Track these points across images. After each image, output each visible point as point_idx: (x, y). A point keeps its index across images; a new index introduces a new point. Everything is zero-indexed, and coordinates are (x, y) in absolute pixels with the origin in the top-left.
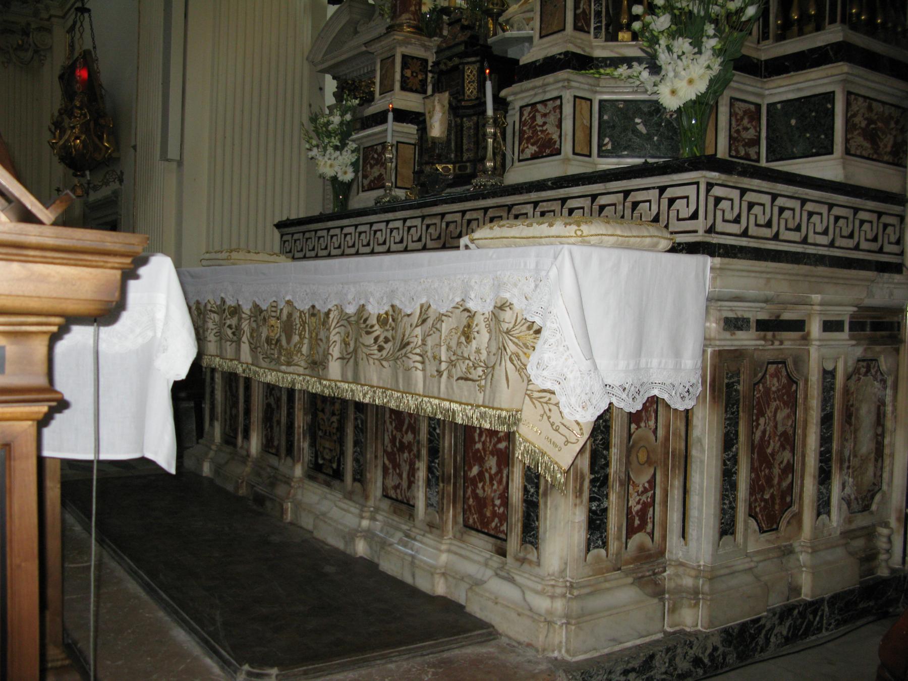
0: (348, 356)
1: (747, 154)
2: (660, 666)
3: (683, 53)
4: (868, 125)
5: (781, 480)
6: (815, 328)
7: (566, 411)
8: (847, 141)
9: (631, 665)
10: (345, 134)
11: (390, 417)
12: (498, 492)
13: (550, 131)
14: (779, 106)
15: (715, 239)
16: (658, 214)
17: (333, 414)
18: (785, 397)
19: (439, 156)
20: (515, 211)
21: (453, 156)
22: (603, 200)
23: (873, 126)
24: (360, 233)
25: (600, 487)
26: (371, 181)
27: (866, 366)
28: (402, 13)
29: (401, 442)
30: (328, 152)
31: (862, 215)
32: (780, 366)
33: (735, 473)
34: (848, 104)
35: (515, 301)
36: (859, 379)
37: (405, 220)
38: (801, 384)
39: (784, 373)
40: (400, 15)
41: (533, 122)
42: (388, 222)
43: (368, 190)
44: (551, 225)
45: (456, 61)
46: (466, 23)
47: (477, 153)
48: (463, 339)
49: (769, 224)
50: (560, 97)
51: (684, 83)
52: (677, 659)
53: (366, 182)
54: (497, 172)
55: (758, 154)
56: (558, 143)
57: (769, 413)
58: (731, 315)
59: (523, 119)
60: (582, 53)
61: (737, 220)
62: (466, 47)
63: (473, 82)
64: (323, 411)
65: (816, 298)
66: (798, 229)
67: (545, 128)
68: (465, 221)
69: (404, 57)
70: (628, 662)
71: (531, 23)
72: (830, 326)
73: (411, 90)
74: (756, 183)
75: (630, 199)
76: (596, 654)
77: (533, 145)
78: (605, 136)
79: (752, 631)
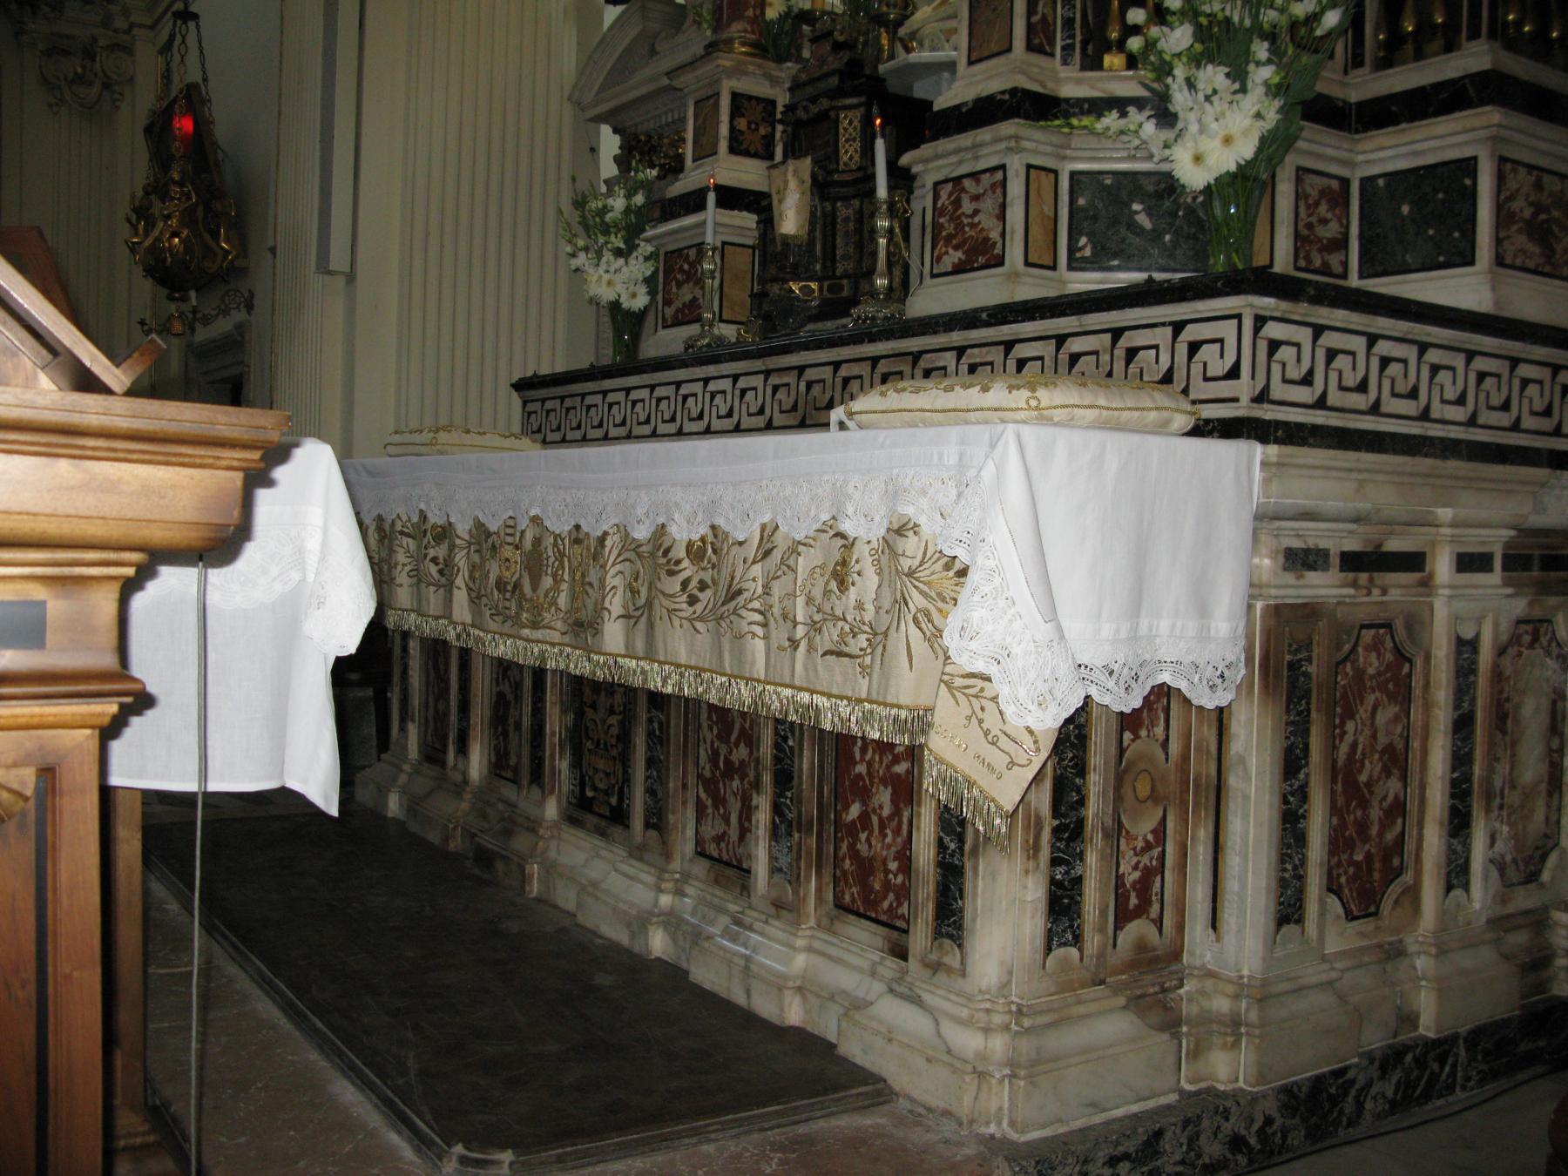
0: (637, 613)
1: (1326, 265)
2: (1173, 1149)
3: (1215, 92)
4: (1535, 215)
5: (1384, 827)
6: (1442, 566)
7: (1009, 711)
8: (1499, 241)
9: (1121, 1149)
10: (633, 229)
11: (710, 718)
12: (894, 849)
13: (984, 225)
14: (1381, 182)
15: (1268, 413)
16: (1171, 370)
17: (612, 712)
18: (1391, 686)
19: (795, 266)
20: (924, 363)
21: (818, 267)
22: (1075, 345)
23: (1543, 216)
24: (659, 400)
25: (1070, 840)
26: (678, 310)
27: (1533, 630)
28: (731, 20)
29: (728, 762)
30: (604, 259)
31: (1525, 371)
32: (1382, 631)
33: (1304, 817)
34: (1501, 178)
35: (922, 520)
36: (1520, 654)
37: (736, 378)
38: (1419, 663)
39: (1389, 644)
40: (728, 25)
41: (956, 210)
42: (706, 381)
43: (673, 325)
44: (985, 389)
45: (825, 103)
46: (841, 39)
47: (859, 262)
48: (833, 585)
49: (1362, 387)
50: (1003, 167)
51: (1216, 143)
52: (1203, 1138)
53: (669, 311)
54: (895, 295)
55: (1345, 264)
56: (999, 245)
57: (1363, 712)
58: (1297, 544)
59: (939, 204)
60: (1041, 90)
61: (1307, 380)
62: (841, 80)
63: (854, 140)
64: (593, 707)
65: (1445, 514)
66: (1413, 394)
67: (976, 220)
68: (839, 380)
69: (736, 97)
70: (1117, 1144)
71: (954, 39)
72: (1469, 563)
73: (747, 154)
74: (1340, 316)
75: (1125, 342)
76: (1061, 1130)
77: (956, 248)
78: (1081, 234)
79: (1333, 1091)
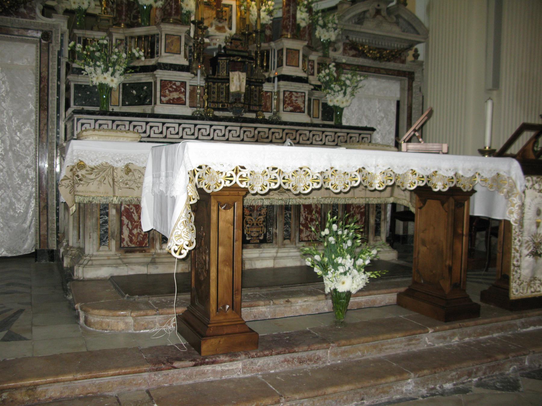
11: (304, 210)
22: (339, 134)
50: (305, 93)
75: (349, 135)
77: (291, 106)
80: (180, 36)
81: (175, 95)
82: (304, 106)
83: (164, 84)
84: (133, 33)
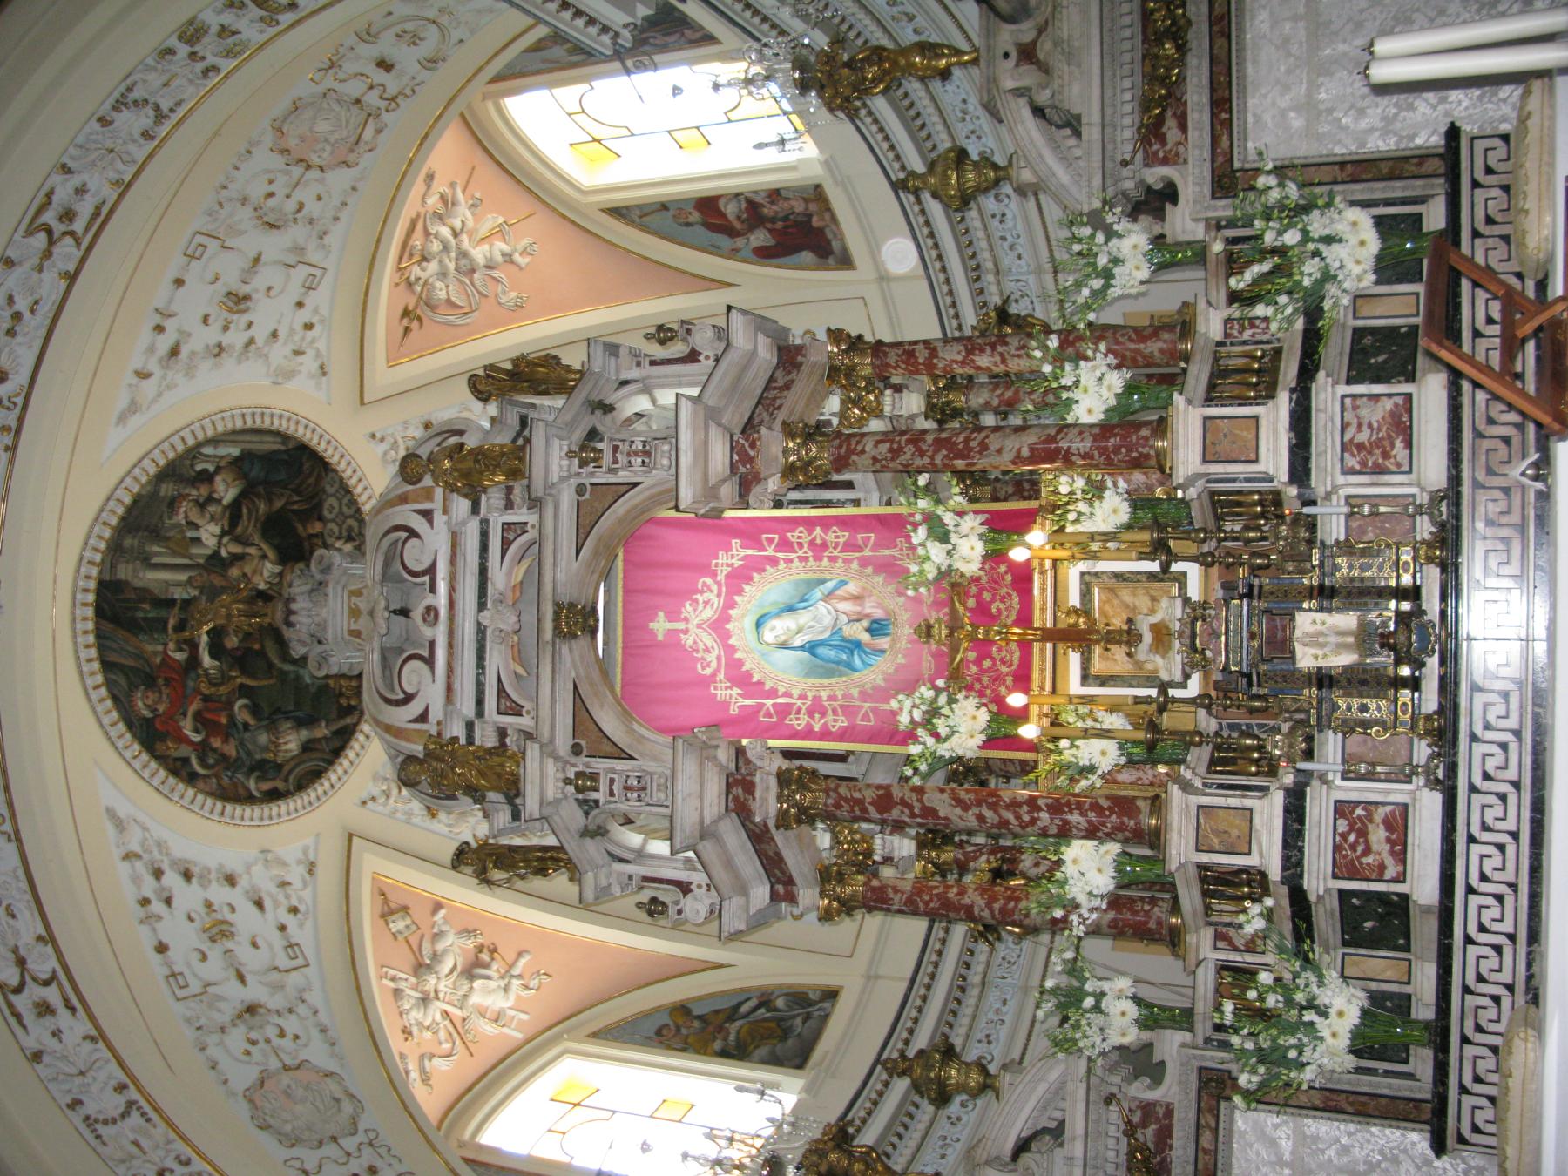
13: (1379, 417)
50: (1343, 397)
59: (1358, 467)
67: (1375, 425)
75: (1481, 227)
77: (1393, 446)
80: (1199, 807)
81: (1378, 836)
82: (1390, 395)
83: (1344, 867)
84: (1194, 913)
